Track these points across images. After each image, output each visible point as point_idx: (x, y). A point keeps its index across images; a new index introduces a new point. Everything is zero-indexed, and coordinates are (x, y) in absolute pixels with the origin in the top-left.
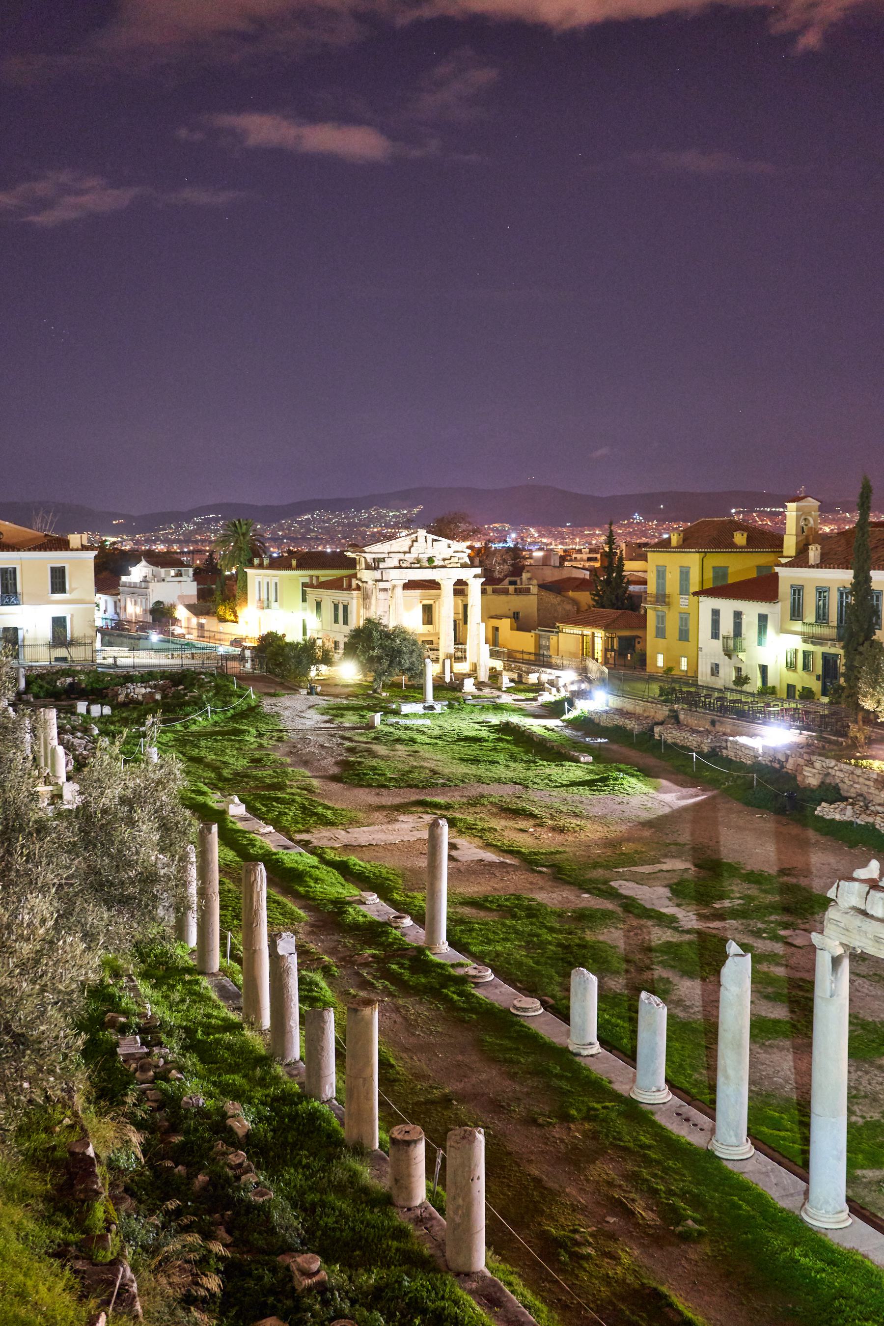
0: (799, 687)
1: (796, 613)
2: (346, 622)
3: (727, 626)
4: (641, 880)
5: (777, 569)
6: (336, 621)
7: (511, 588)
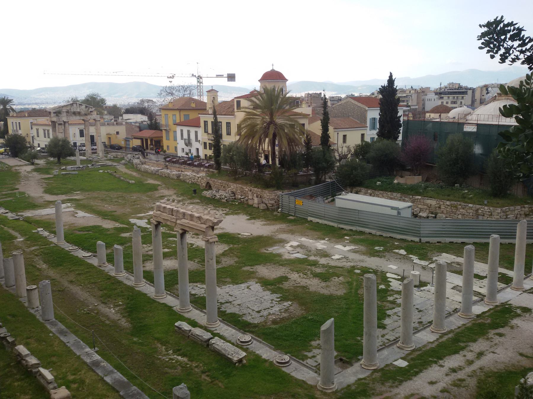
0: (208, 156)
1: (206, 131)
2: (49, 137)
3: (185, 136)
4: (140, 218)
5: (200, 115)
6: (45, 137)
7: (115, 123)
